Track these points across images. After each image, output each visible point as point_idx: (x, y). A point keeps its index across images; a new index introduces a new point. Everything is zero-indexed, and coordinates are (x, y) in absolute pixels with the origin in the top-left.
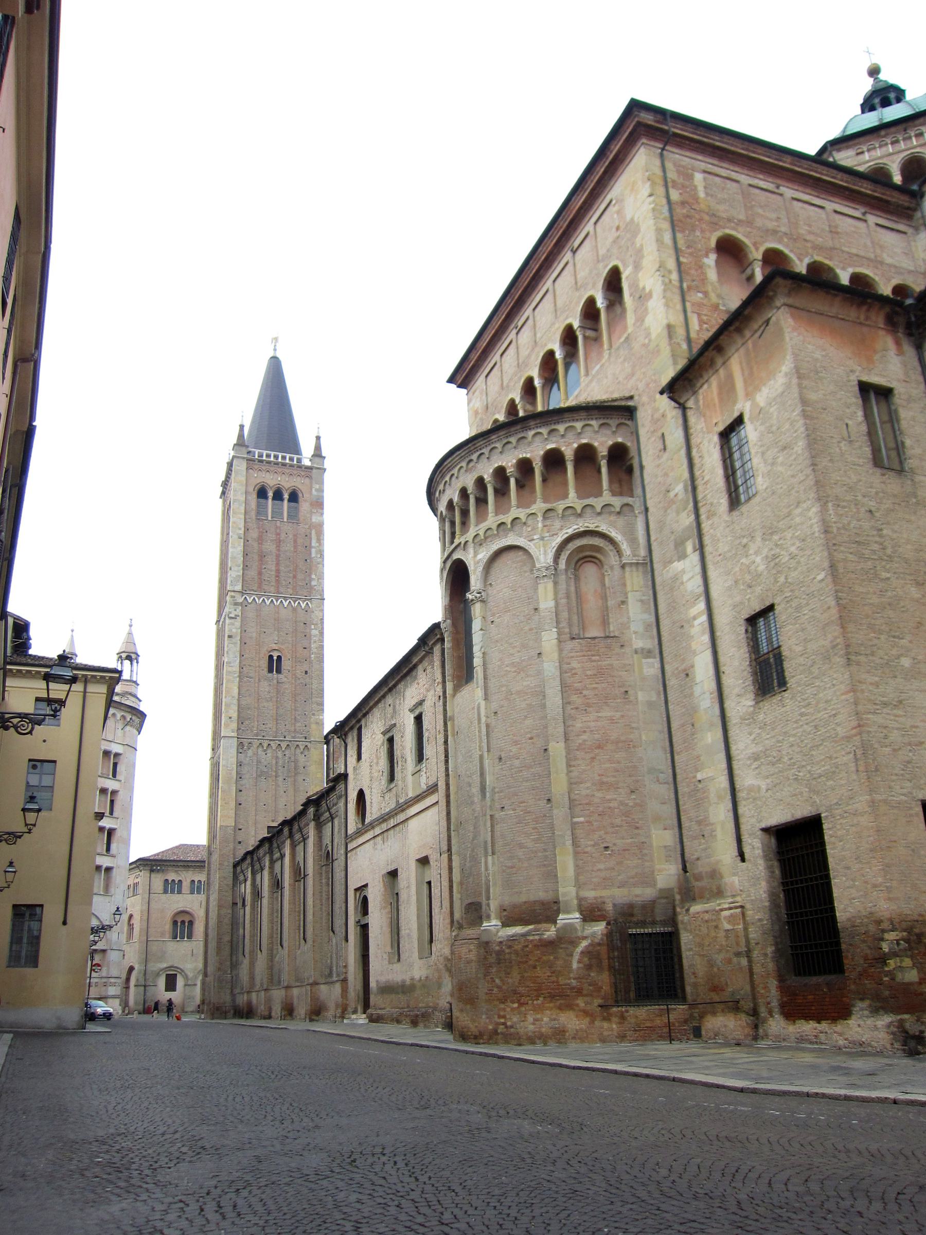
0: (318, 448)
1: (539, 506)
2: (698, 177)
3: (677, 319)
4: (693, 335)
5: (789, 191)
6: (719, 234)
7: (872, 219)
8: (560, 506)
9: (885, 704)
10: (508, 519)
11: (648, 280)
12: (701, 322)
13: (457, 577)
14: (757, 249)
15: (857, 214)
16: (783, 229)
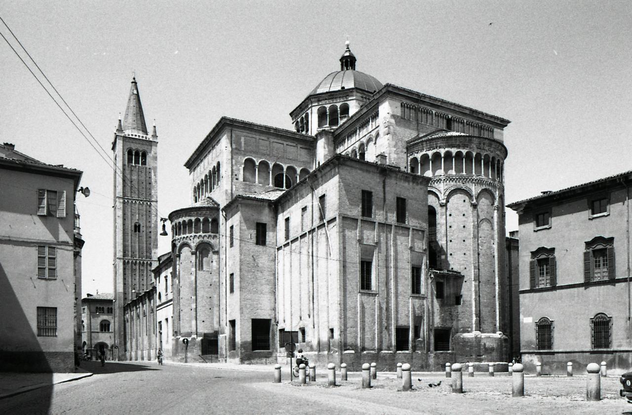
0: (155, 132)
1: (193, 234)
2: (243, 140)
3: (229, 188)
4: (233, 192)
5: (272, 140)
6: (246, 158)
7: (299, 146)
8: (198, 235)
9: (247, 299)
10: (185, 236)
11: (225, 171)
12: (236, 188)
13: (174, 246)
14: (257, 161)
15: (295, 145)
16: (268, 153)
